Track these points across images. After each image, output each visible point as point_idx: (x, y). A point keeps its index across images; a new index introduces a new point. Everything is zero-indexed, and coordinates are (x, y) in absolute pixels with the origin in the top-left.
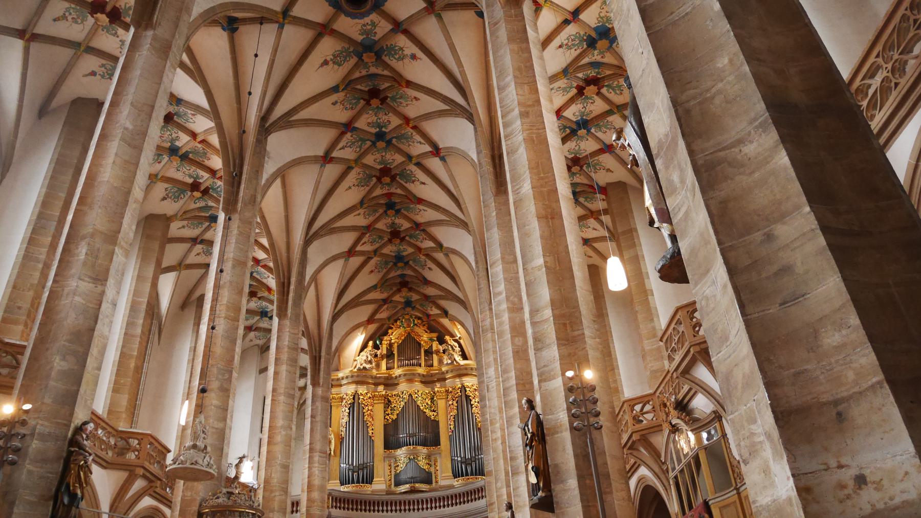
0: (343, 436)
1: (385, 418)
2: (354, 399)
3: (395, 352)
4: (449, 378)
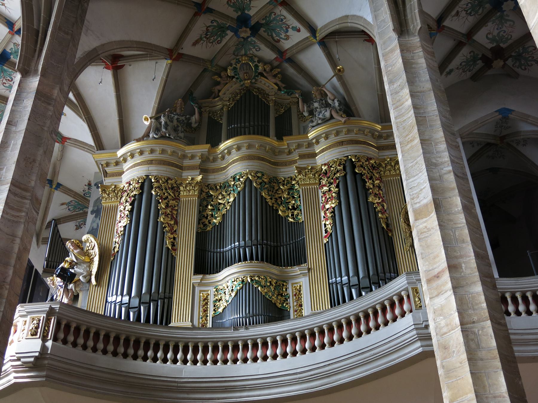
0: (116, 250)
1: (199, 223)
2: (142, 187)
3: (224, 122)
4: (322, 151)
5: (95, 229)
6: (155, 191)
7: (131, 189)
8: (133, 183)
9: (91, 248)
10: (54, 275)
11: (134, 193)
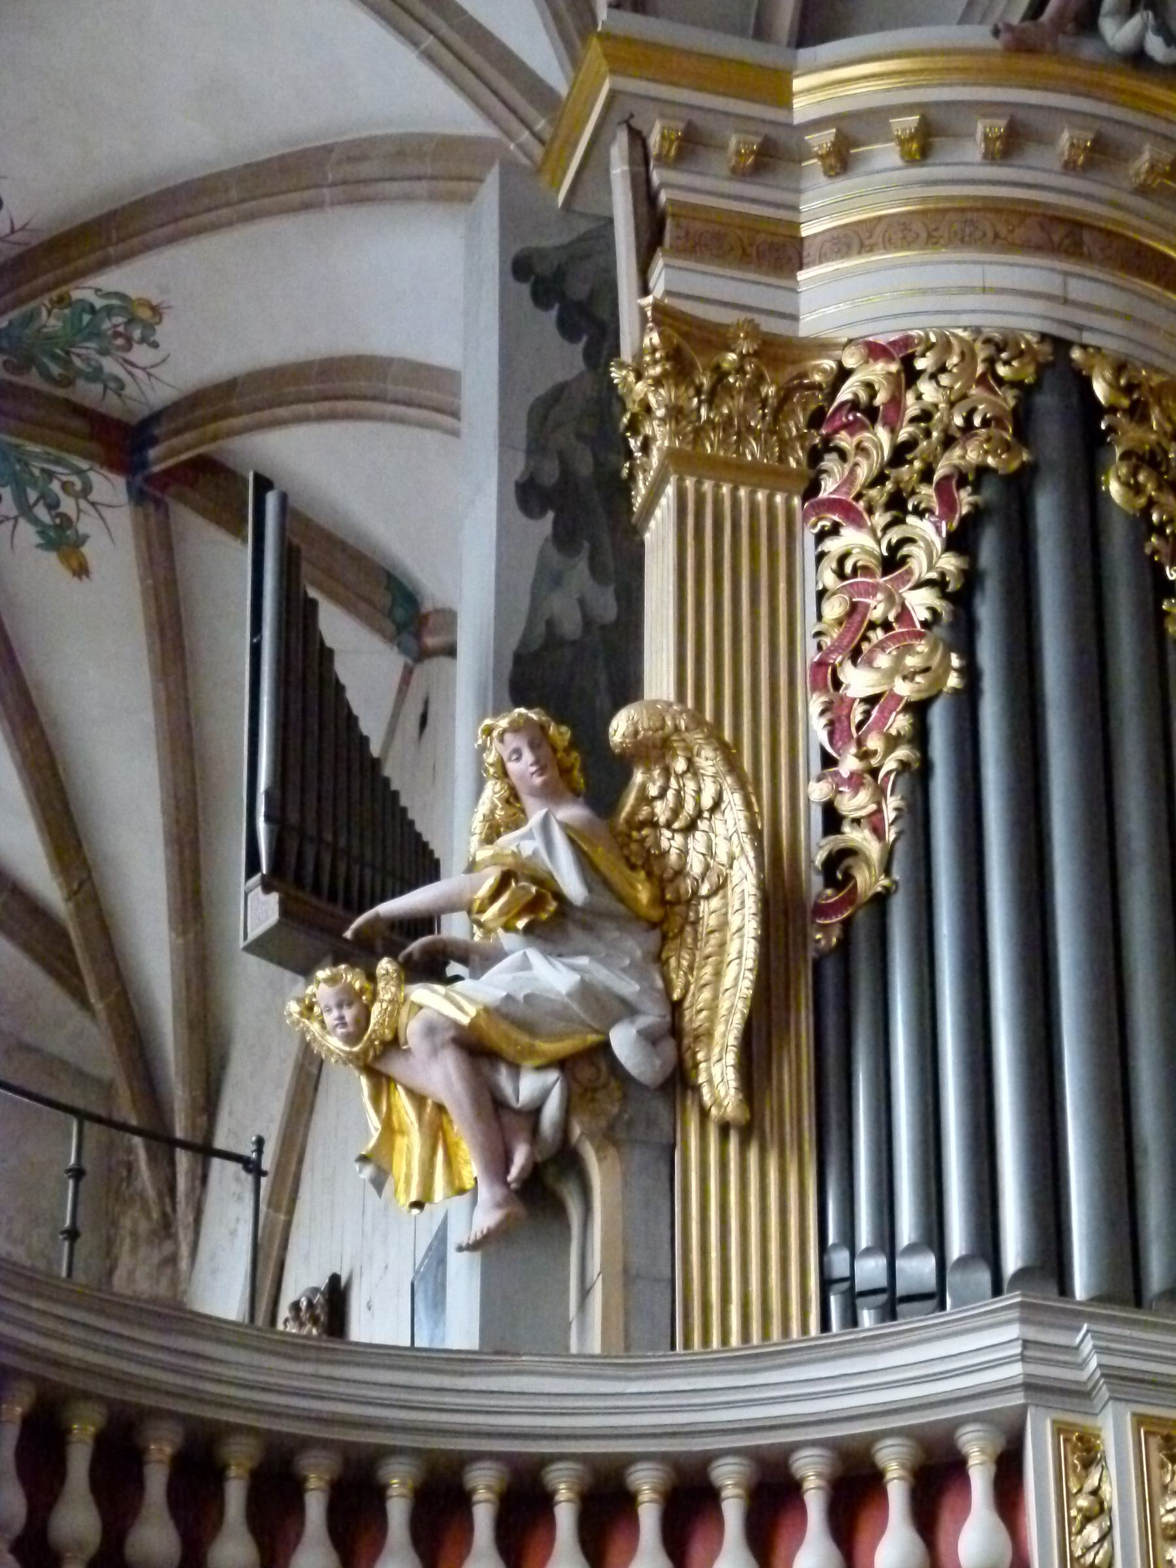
0: (867, 880)
5: (573, 643)
6: (1125, 484)
7: (925, 416)
8: (943, 369)
9: (676, 812)
10: (385, 965)
11: (971, 454)
